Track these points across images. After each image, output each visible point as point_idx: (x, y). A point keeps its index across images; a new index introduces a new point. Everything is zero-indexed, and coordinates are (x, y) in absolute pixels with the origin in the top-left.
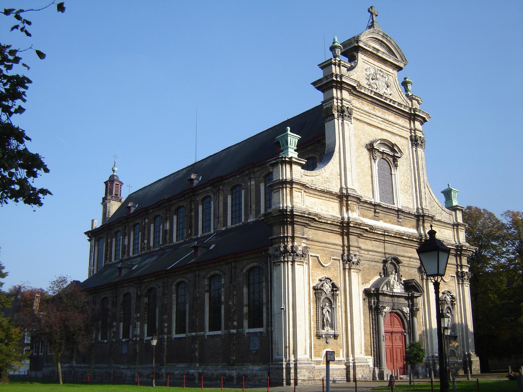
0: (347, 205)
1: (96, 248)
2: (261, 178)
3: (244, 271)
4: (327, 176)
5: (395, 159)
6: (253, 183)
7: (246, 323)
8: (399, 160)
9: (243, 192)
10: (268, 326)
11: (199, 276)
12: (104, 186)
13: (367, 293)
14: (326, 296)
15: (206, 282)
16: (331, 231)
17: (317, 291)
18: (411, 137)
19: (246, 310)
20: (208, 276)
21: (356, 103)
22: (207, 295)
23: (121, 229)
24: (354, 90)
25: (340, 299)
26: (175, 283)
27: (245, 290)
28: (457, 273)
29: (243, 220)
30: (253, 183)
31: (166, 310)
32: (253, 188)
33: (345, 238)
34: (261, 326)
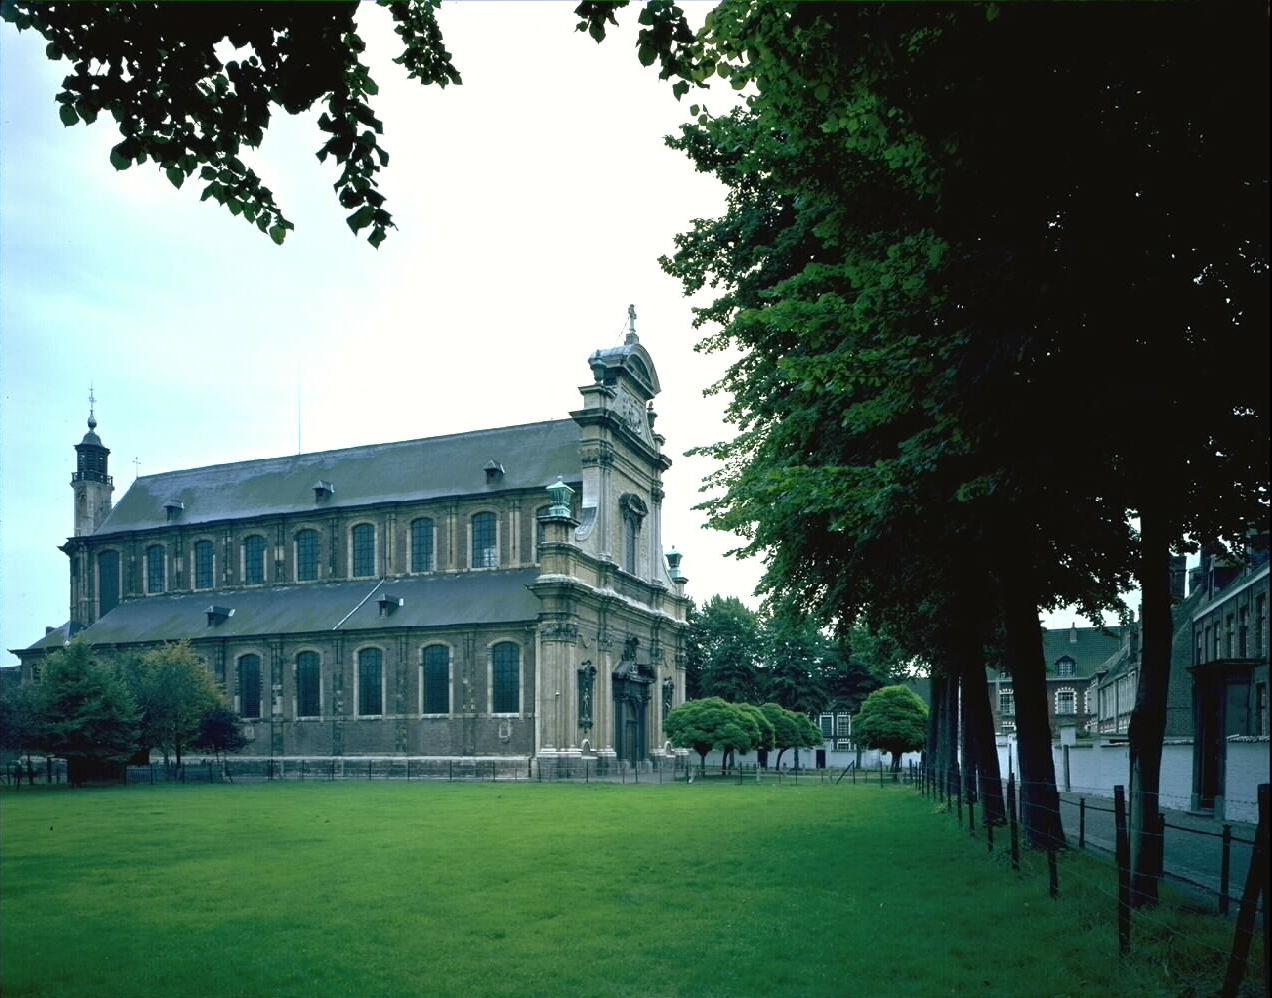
0: (606, 577)
1: (96, 567)
2: (469, 517)
3: (490, 645)
4: (582, 537)
5: (640, 518)
6: (454, 520)
7: (490, 707)
8: (644, 520)
9: (435, 530)
10: (525, 710)
11: (407, 644)
12: (76, 453)
13: (615, 677)
14: (586, 677)
15: (420, 652)
16: (592, 608)
17: (580, 673)
18: (653, 489)
19: (490, 691)
20: (423, 645)
21: (622, 451)
22: (421, 669)
23: (164, 543)
24: (616, 435)
25: (595, 684)
26: (358, 649)
27: (490, 668)
28: (676, 657)
29: (435, 569)
30: (454, 520)
31: (340, 682)
32: (454, 527)
33: (602, 615)
34: (518, 711)
